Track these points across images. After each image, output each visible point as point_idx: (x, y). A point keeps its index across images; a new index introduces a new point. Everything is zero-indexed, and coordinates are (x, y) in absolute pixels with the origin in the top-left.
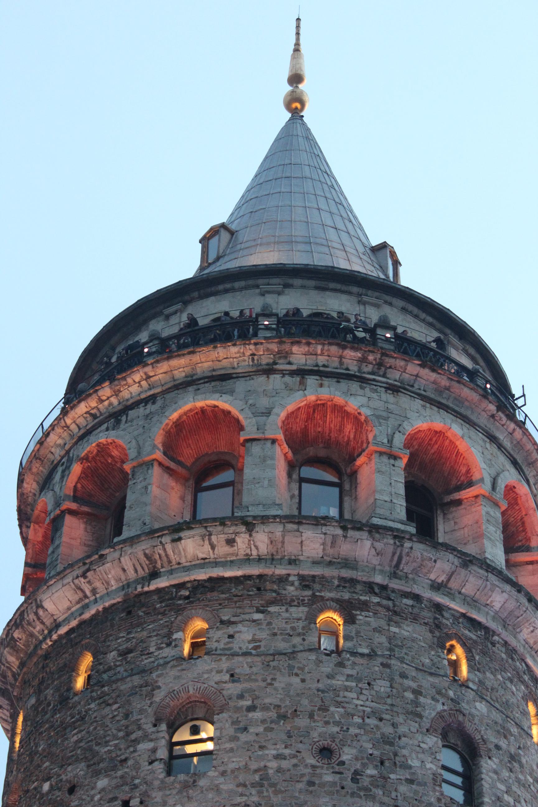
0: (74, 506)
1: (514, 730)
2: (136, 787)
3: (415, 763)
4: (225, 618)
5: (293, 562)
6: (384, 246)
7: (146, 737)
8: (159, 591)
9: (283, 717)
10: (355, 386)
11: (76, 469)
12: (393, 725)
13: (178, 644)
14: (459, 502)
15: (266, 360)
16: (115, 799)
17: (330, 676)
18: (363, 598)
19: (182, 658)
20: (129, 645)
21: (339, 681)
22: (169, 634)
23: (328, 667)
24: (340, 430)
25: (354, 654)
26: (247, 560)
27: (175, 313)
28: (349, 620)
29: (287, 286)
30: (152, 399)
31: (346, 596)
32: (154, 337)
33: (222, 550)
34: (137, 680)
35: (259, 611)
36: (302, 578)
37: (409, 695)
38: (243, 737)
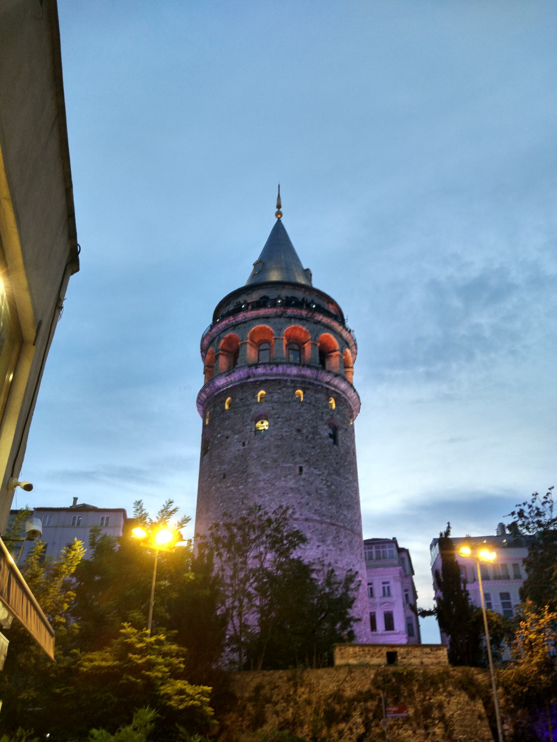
0: (222, 352)
1: (346, 422)
2: (246, 439)
3: (322, 433)
4: (270, 391)
5: (289, 375)
6: (308, 270)
7: (248, 425)
8: (250, 382)
9: (287, 420)
10: (305, 322)
11: (222, 341)
12: (317, 423)
13: (257, 398)
14: (332, 356)
15: (280, 313)
16: (240, 442)
17: (300, 409)
18: (308, 386)
19: (257, 402)
20: (243, 397)
21: (302, 410)
22: (254, 395)
23: (298, 407)
24: (300, 334)
25: (306, 403)
26: (276, 375)
27: (250, 293)
28: (304, 393)
29: (284, 287)
30: (245, 322)
31: (303, 386)
32: (245, 302)
33: (269, 371)
34: (245, 408)
35: (280, 389)
36: (291, 380)
37: (320, 414)
38: (277, 426)
